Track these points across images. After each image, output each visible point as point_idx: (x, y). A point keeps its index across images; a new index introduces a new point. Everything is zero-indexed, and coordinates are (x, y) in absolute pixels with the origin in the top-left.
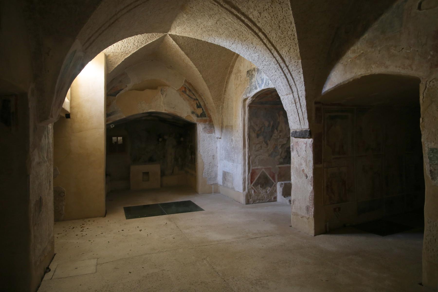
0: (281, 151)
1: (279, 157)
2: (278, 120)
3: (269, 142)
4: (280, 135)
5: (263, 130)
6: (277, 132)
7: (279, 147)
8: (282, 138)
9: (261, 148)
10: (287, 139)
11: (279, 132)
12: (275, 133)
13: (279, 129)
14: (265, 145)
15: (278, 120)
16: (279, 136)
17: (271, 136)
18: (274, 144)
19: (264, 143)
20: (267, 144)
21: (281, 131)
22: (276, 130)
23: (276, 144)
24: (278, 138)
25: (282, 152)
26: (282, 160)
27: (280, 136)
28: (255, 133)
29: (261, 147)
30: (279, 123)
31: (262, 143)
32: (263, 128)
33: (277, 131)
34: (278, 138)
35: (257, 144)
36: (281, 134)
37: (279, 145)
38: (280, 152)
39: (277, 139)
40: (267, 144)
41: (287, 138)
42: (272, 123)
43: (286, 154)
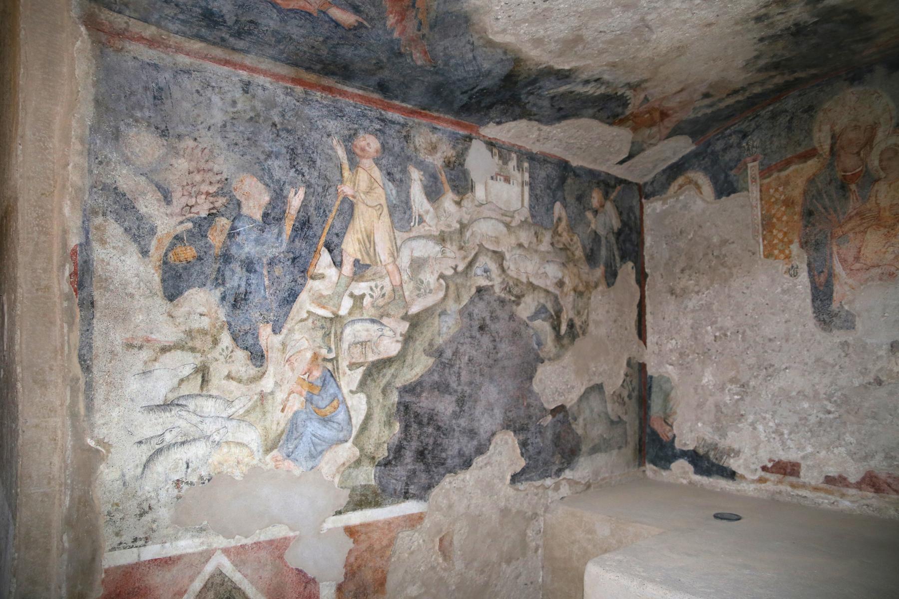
0: (364, 408)
1: (346, 452)
2: (347, 189)
3: (266, 334)
4: (352, 295)
5: (216, 239)
6: (332, 272)
7: (350, 380)
8: (373, 321)
9: (205, 381)
10: (405, 326)
11: (347, 269)
12: (322, 277)
13: (351, 247)
14: (241, 361)
15: (347, 189)
16: (347, 304)
17: (291, 297)
18: (309, 355)
19: (226, 340)
20: (258, 357)
21: (361, 269)
22: (325, 257)
23: (325, 360)
24: (343, 312)
25: (368, 417)
26: (367, 475)
27: (358, 300)
28: (145, 253)
29: (203, 373)
30: (348, 209)
31: (216, 342)
32: (223, 222)
33: (338, 264)
34: (343, 312)
35: (164, 350)
36: (361, 288)
37: (352, 366)
38: (358, 420)
39: (336, 318)
40: (258, 357)
41: (405, 318)
42: (296, 199)
43: (397, 427)
